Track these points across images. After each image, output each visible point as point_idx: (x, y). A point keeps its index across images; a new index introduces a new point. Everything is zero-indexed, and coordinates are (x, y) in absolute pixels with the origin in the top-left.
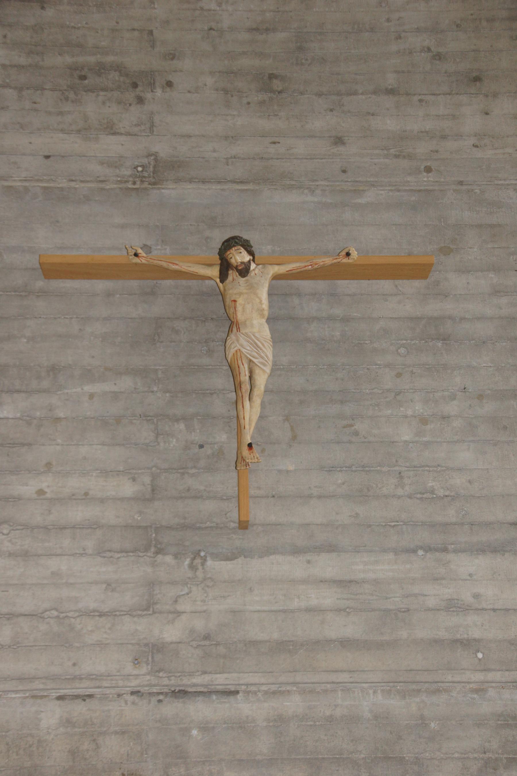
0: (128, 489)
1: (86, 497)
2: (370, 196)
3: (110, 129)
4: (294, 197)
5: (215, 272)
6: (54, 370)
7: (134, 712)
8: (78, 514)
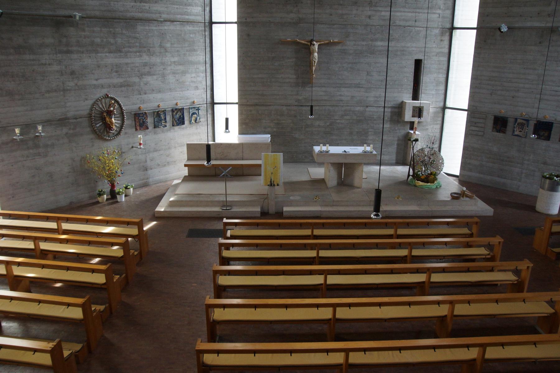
0: (295, 77)
2: (335, 26)
3: (292, 12)
4: (322, 26)
5: (309, 44)
7: (295, 108)
8: (287, 80)
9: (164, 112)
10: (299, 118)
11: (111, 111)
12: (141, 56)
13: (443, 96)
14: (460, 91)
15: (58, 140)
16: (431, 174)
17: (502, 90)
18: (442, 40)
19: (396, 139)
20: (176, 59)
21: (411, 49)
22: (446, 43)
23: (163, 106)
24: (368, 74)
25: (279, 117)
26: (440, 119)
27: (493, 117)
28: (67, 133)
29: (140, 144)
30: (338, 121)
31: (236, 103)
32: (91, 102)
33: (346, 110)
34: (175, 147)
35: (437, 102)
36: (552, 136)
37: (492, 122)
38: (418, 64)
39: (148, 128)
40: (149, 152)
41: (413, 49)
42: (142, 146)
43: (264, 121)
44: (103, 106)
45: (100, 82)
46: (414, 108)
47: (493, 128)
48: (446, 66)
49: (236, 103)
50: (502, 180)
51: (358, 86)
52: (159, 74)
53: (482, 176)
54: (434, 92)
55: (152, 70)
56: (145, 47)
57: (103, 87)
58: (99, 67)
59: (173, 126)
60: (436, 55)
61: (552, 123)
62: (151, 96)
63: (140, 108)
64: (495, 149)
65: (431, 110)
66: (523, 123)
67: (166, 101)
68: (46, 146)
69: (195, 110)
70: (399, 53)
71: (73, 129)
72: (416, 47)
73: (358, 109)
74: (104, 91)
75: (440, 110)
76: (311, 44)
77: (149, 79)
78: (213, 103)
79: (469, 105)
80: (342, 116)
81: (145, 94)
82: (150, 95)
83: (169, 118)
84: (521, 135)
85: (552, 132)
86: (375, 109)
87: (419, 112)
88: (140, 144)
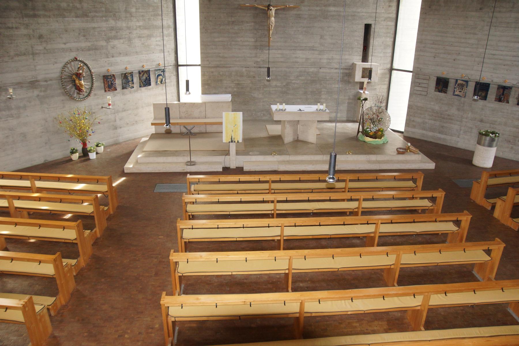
0: (253, 40)
1: (247, 41)
5: (266, 9)
6: (242, 22)
7: (253, 69)
8: (246, 43)
9: (131, 74)
10: (257, 78)
11: (80, 74)
12: (107, 21)
13: (390, 59)
14: (406, 54)
15: (30, 102)
16: (379, 130)
17: (444, 54)
18: (390, 6)
19: (347, 98)
20: (141, 23)
21: (361, 14)
22: (394, 8)
23: (130, 69)
24: (322, 37)
25: (239, 78)
26: (387, 80)
27: (436, 79)
28: (38, 96)
29: (109, 105)
30: (294, 81)
31: (199, 65)
32: (61, 65)
33: (301, 72)
34: (142, 107)
35: (384, 64)
36: (488, 96)
37: (435, 83)
38: (368, 28)
39: (116, 90)
40: (118, 112)
41: (363, 14)
42: (111, 107)
43: (225, 82)
44: (73, 68)
45: (68, 46)
46: (364, 70)
47: (436, 88)
48: (393, 30)
49: (199, 65)
50: (442, 136)
51: (312, 49)
52: (125, 38)
53: (424, 132)
54: (382, 55)
55: (119, 34)
56: (111, 12)
57: (71, 50)
58: (66, 31)
59: (140, 87)
60: (385, 20)
61: (489, 84)
62: (118, 59)
63: (108, 70)
64: (437, 108)
65: (379, 72)
66: (463, 84)
67: (133, 63)
68: (18, 108)
69: (161, 72)
70: (350, 18)
71: (44, 91)
72: (366, 13)
73: (311, 70)
74: (73, 55)
75: (387, 72)
76: (268, 9)
77: (115, 42)
78: (177, 66)
79: (414, 67)
80: (298, 76)
81: (113, 57)
82: (116, 58)
83: (136, 79)
84: (461, 95)
85: (489, 92)
86: (328, 71)
87: (368, 73)
88: (109, 105)
